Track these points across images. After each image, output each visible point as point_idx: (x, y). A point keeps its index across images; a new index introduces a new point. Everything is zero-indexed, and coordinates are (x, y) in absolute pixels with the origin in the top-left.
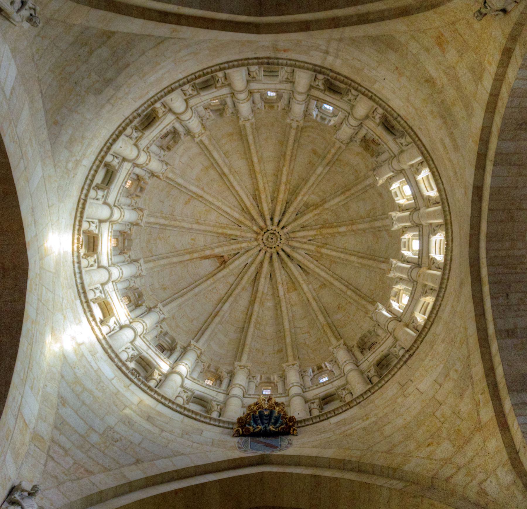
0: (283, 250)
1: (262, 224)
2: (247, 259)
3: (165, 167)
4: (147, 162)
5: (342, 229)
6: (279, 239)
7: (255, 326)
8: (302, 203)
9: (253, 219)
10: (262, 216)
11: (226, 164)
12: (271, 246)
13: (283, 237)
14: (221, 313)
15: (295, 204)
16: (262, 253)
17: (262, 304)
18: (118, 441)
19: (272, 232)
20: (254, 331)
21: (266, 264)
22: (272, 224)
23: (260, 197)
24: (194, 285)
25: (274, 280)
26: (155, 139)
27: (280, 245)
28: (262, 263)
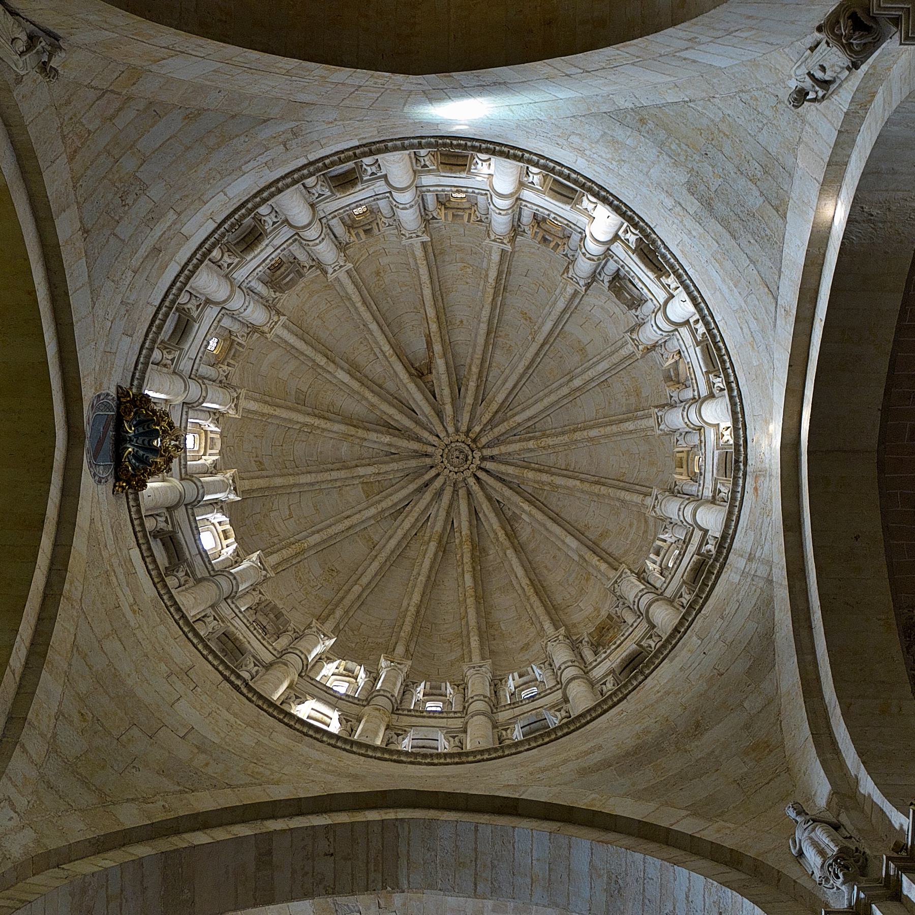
0: (438, 475)
1: (484, 441)
3: (582, 283)
4: (588, 256)
5: (468, 579)
6: (456, 470)
9: (491, 423)
11: (587, 383)
14: (331, 367)
15: (517, 499)
16: (432, 439)
17: (346, 436)
18: (122, 200)
19: (470, 458)
23: (530, 439)
24: (382, 322)
25: (387, 459)
28: (418, 439)
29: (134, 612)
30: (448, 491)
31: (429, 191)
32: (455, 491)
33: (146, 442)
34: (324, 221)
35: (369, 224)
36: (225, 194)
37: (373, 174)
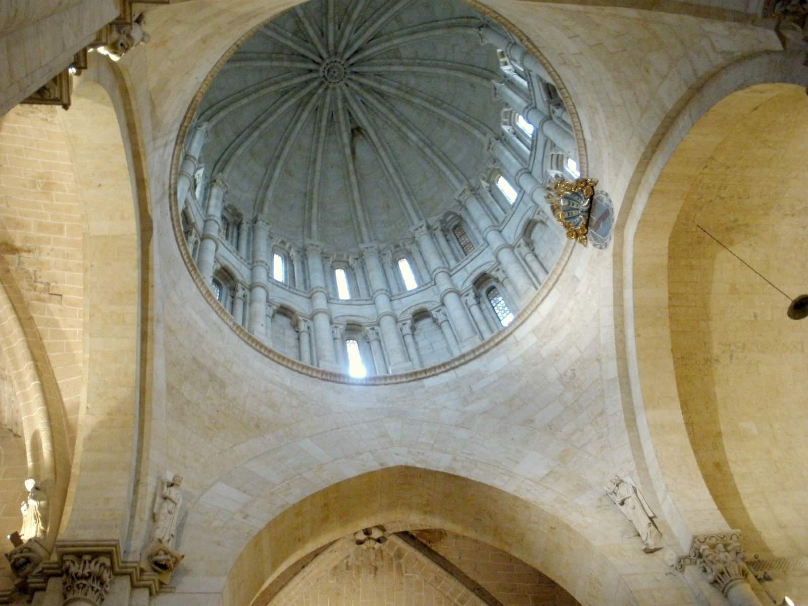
0: (348, 59)
1: (316, 83)
2: (356, 101)
3: (260, 223)
4: (264, 264)
6: (335, 64)
7: (439, 106)
8: (295, 38)
9: (311, 94)
10: (307, 83)
11: (250, 134)
12: (343, 74)
13: (333, 59)
15: (295, 47)
16: (351, 84)
18: (574, 374)
19: (326, 72)
20: (444, 109)
21: (363, 80)
22: (317, 71)
25: (384, 73)
26: (239, 257)
27: (343, 62)
28: (361, 85)
29: (596, 109)
30: (341, 49)
31: (366, 300)
32: (336, 47)
33: (571, 204)
34: (433, 283)
35: (396, 252)
36: (508, 359)
37: (404, 324)
